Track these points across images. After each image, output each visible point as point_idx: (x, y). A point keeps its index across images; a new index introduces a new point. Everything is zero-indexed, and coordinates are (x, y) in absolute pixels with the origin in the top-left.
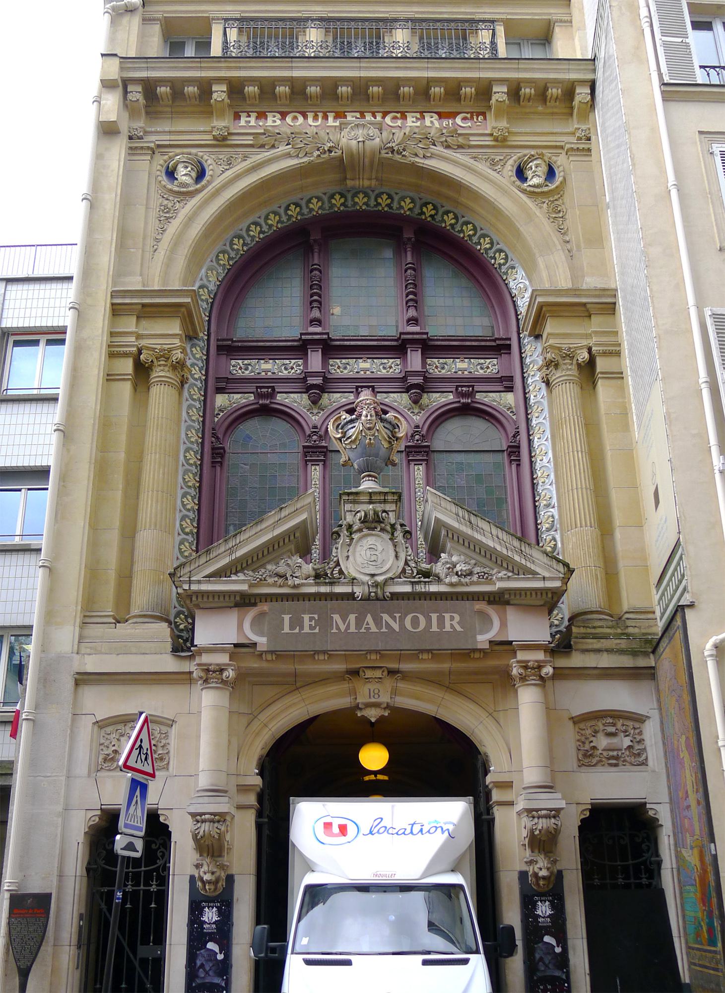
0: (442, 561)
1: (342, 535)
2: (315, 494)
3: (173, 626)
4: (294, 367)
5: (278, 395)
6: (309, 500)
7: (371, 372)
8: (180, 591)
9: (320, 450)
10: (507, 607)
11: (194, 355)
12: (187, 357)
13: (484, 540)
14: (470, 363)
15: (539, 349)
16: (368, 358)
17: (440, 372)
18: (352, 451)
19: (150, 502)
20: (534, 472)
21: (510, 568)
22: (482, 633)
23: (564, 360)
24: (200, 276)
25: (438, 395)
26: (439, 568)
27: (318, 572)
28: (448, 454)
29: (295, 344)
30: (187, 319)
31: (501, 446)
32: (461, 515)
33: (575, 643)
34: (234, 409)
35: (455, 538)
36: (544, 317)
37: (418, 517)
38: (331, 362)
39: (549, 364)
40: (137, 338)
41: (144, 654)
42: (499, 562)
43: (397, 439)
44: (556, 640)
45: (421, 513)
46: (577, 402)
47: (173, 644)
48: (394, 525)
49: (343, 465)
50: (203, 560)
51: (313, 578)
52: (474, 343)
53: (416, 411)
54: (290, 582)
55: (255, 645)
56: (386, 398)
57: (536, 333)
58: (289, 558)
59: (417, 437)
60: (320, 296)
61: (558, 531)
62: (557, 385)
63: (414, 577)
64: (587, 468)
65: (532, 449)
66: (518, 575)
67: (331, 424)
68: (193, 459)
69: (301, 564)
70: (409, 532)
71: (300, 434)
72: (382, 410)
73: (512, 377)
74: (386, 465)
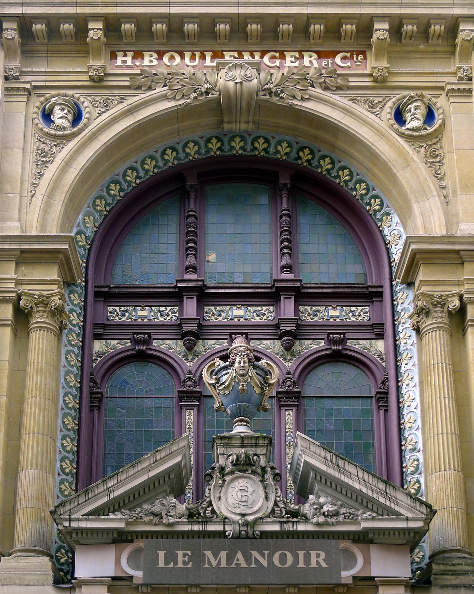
0: (311, 502)
1: (214, 477)
2: (190, 437)
3: (54, 560)
4: (170, 313)
5: (154, 341)
6: (183, 443)
7: (245, 319)
8: (60, 528)
9: (194, 395)
10: (372, 546)
11: (72, 301)
12: (66, 304)
13: (350, 482)
14: (341, 311)
15: (411, 297)
16: (242, 305)
17: (312, 319)
18: (226, 397)
19: (31, 443)
20: (401, 417)
21: (375, 509)
22: (346, 569)
23: (435, 308)
24: (78, 221)
25: (309, 342)
26: (307, 509)
27: (192, 511)
28: (318, 400)
29: (171, 291)
30: (65, 266)
31: (370, 392)
32: (329, 458)
33: (435, 579)
34: (111, 355)
35: (323, 481)
36: (417, 264)
37: (287, 460)
38: (206, 309)
39: (420, 312)
40: (16, 285)
41: (27, 585)
42: (364, 503)
43: (269, 385)
44: (416, 576)
45: (290, 456)
46: (446, 349)
47: (54, 577)
48: (265, 467)
49: (216, 410)
50: (82, 499)
51: (186, 517)
52: (346, 291)
53: (288, 358)
54: (164, 521)
55: (132, 578)
56: (259, 345)
57: (409, 281)
58: (165, 498)
59: (288, 383)
60: (195, 243)
61: (423, 474)
62: (427, 333)
63: (283, 517)
64: (454, 414)
65: (400, 395)
66: (383, 515)
67: (205, 370)
68: (72, 402)
69: (175, 503)
70: (279, 475)
71: (174, 378)
72: (255, 357)
73: (383, 324)
74: (258, 410)
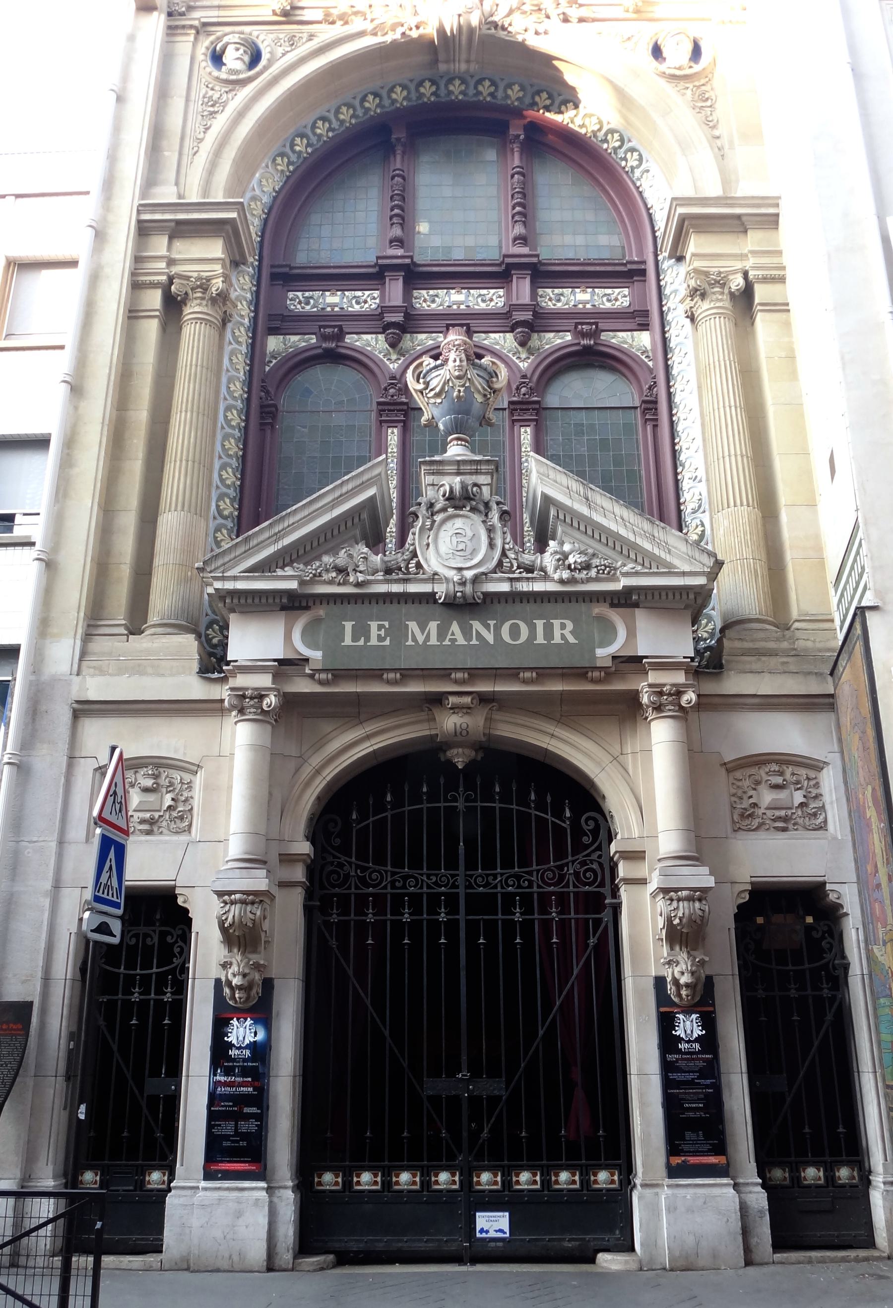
14: (593, 294)
18: (437, 407)
27: (389, 564)
42: (625, 552)
51: (382, 573)
53: (523, 356)
54: (352, 579)
59: (523, 390)
63: (514, 572)
69: (366, 554)
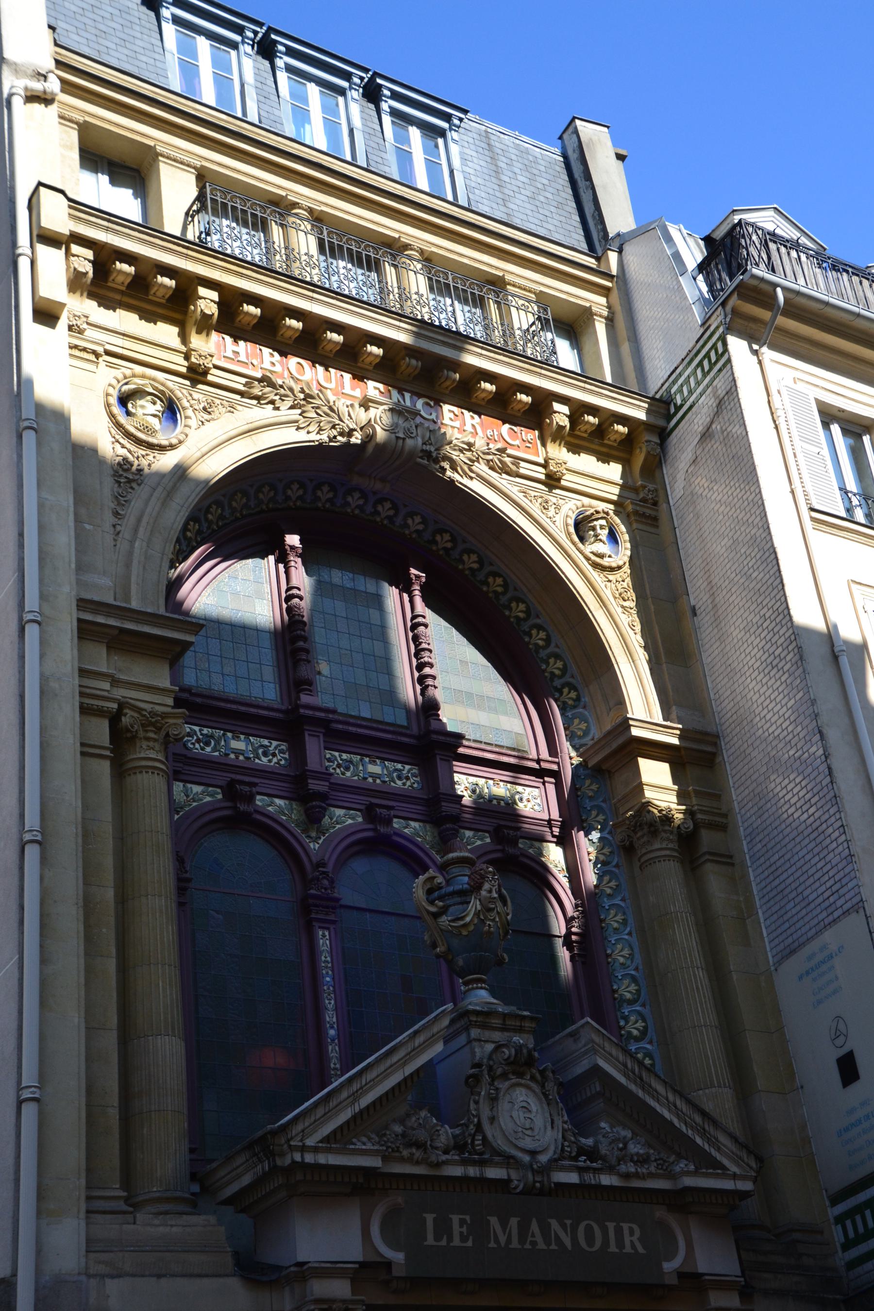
13: (658, 1108)
32: (629, 1065)
55: (388, 1265)
